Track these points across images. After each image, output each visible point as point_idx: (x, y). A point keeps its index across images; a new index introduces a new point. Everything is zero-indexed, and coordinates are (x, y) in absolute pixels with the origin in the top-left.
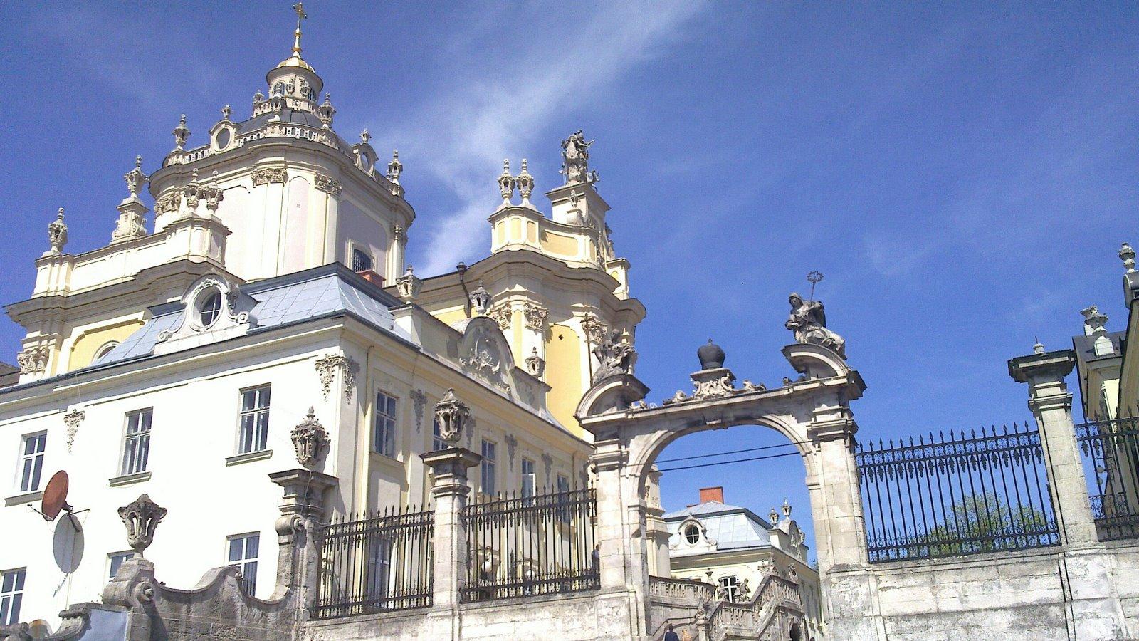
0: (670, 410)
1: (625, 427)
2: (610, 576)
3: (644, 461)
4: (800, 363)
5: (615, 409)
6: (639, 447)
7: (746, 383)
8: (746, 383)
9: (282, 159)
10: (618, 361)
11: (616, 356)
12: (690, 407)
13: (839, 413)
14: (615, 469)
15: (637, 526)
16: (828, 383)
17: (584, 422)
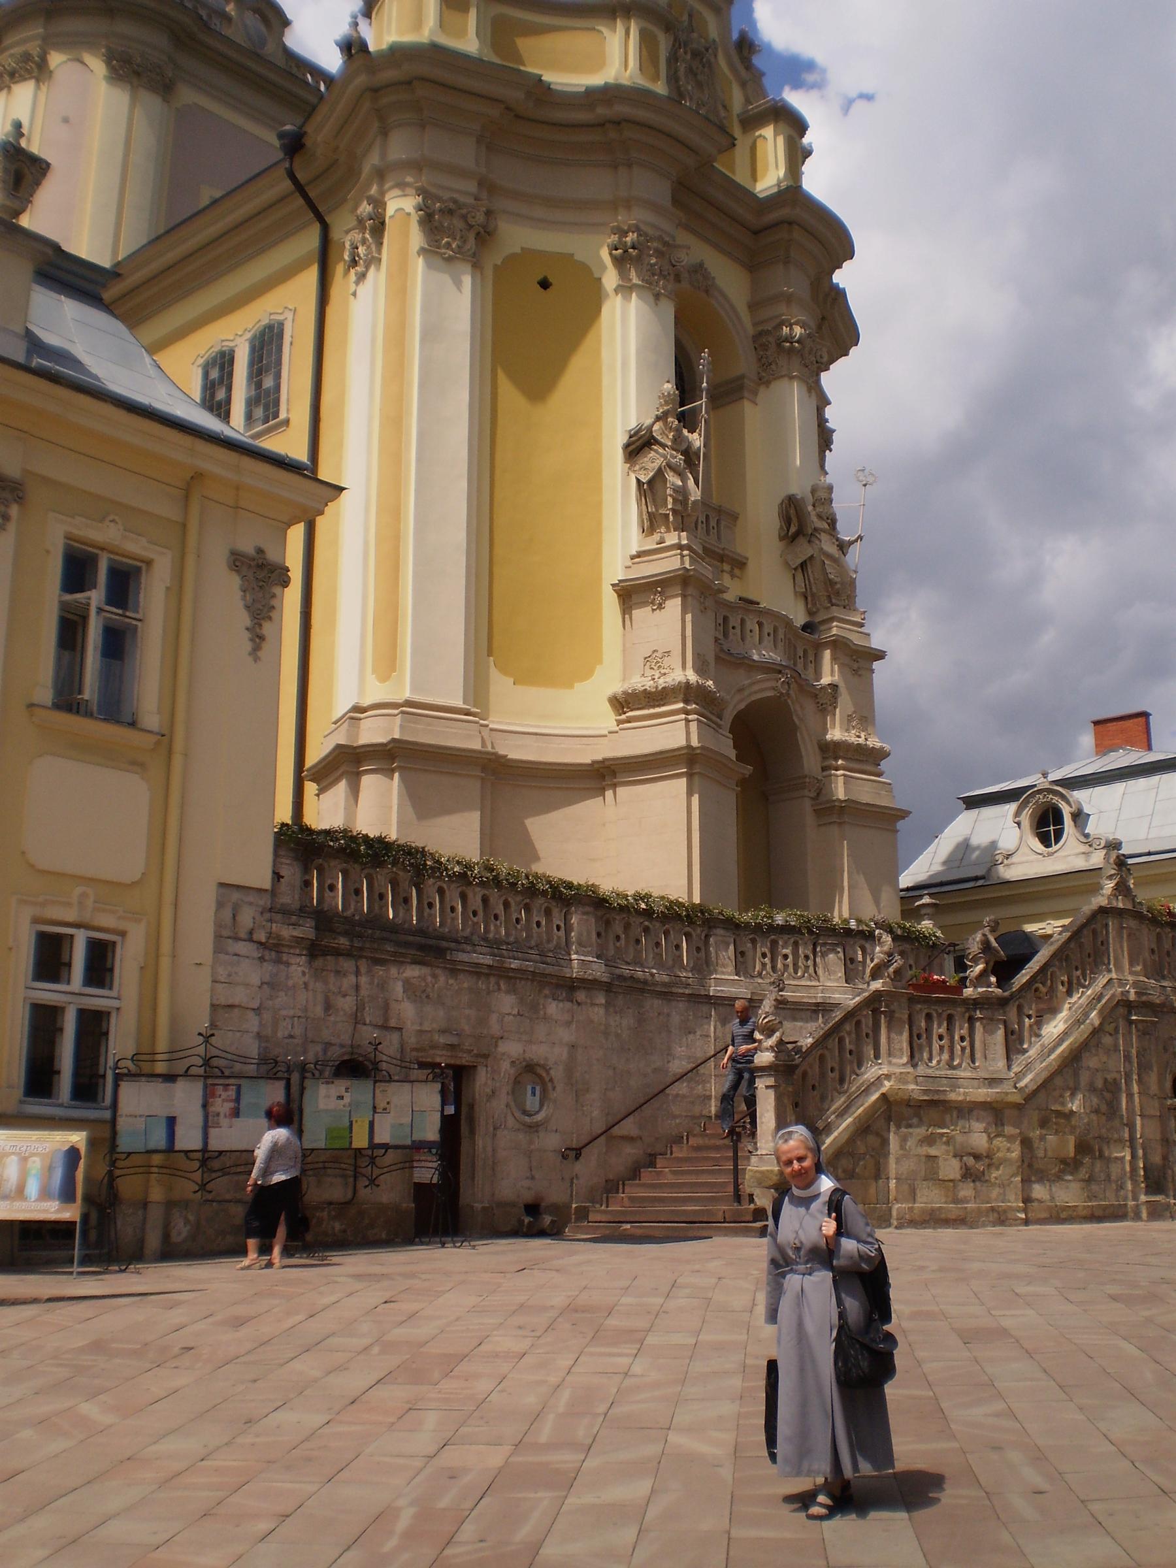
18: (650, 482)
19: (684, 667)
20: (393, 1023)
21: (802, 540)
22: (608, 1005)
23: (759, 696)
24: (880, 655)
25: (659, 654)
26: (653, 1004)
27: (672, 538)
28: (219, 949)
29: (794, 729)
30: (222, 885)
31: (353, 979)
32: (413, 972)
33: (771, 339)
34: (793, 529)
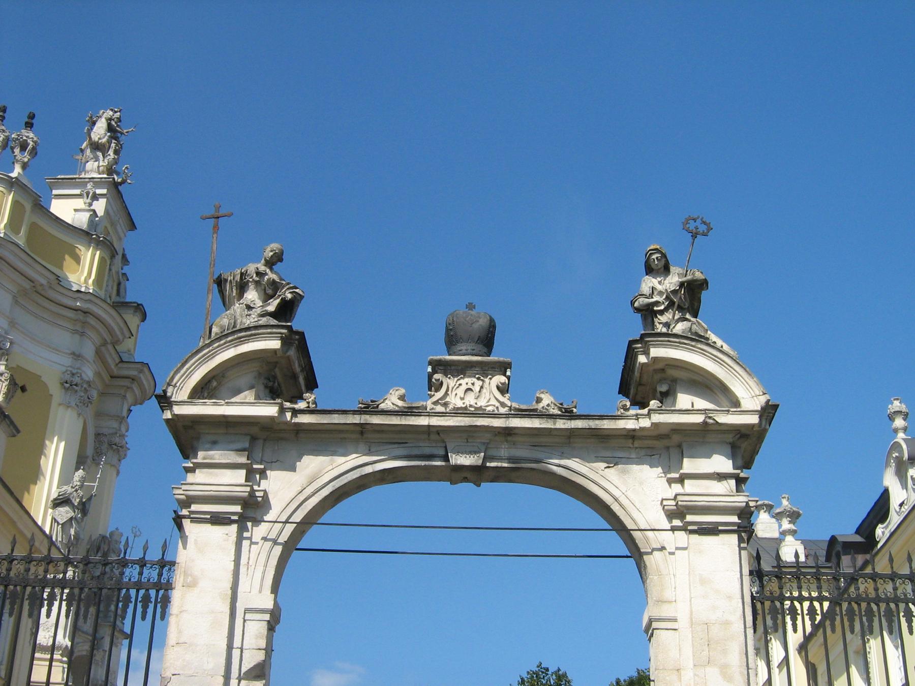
0: (376, 420)
1: (265, 440)
3: (298, 517)
4: (657, 377)
5: (249, 396)
6: (290, 488)
7: (542, 396)
8: (542, 396)
10: (271, 308)
11: (267, 298)
12: (423, 421)
13: (733, 482)
14: (230, 522)
15: (261, 656)
16: (723, 419)
17: (178, 410)
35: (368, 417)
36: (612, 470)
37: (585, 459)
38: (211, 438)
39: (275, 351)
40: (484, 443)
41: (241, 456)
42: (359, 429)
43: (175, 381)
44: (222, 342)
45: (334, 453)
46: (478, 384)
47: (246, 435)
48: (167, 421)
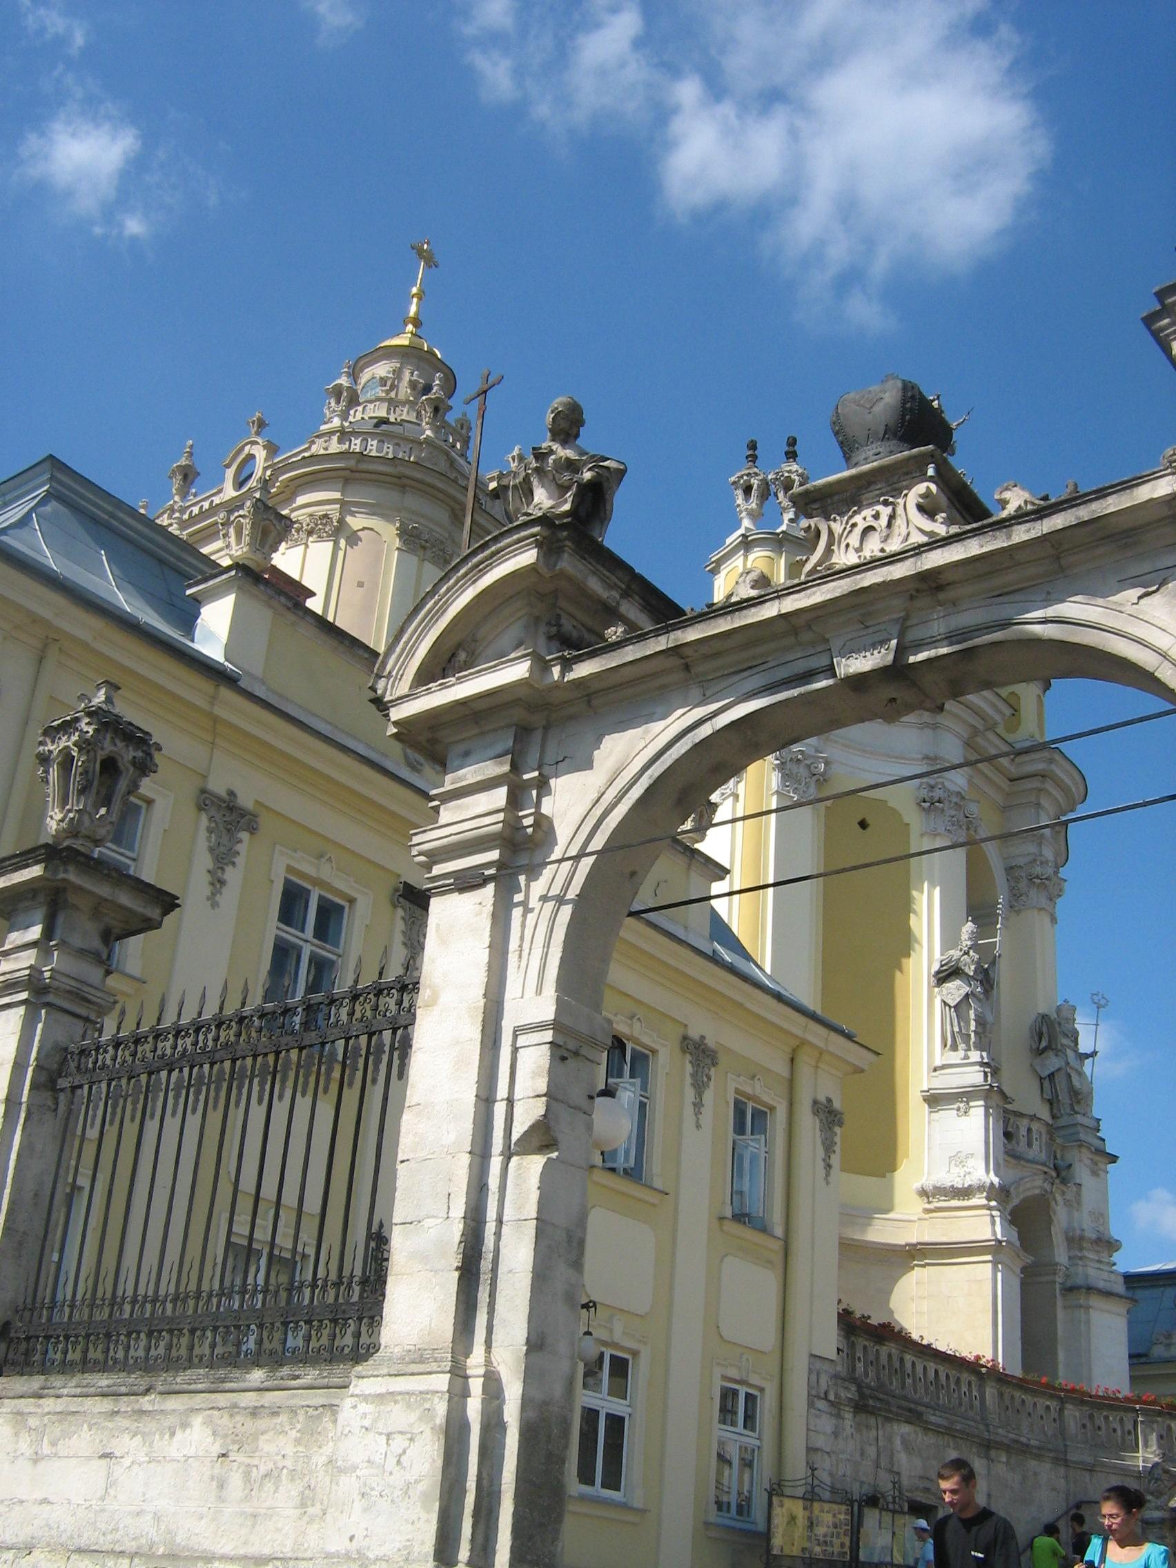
1: (546, 728)
2: (416, 1303)
7: (1007, 495)
8: (1007, 495)
9: (337, 495)
14: (485, 881)
18: (955, 1007)
19: (987, 1171)
20: (895, 1469)
21: (1051, 1054)
22: (1008, 1463)
23: (1029, 1193)
24: (1113, 1159)
25: (963, 1155)
26: (1032, 1464)
27: (975, 1056)
28: (811, 1405)
29: (1049, 1222)
30: (812, 1356)
31: (874, 1431)
32: (906, 1429)
33: (1023, 874)
34: (1044, 1044)
35: (679, 633)
36: (1156, 598)
37: (1095, 591)
38: (461, 748)
39: (531, 569)
40: (897, 620)
41: (501, 764)
42: (674, 661)
43: (388, 668)
44: (452, 581)
45: (650, 718)
46: (885, 511)
47: (508, 726)
48: (394, 735)
